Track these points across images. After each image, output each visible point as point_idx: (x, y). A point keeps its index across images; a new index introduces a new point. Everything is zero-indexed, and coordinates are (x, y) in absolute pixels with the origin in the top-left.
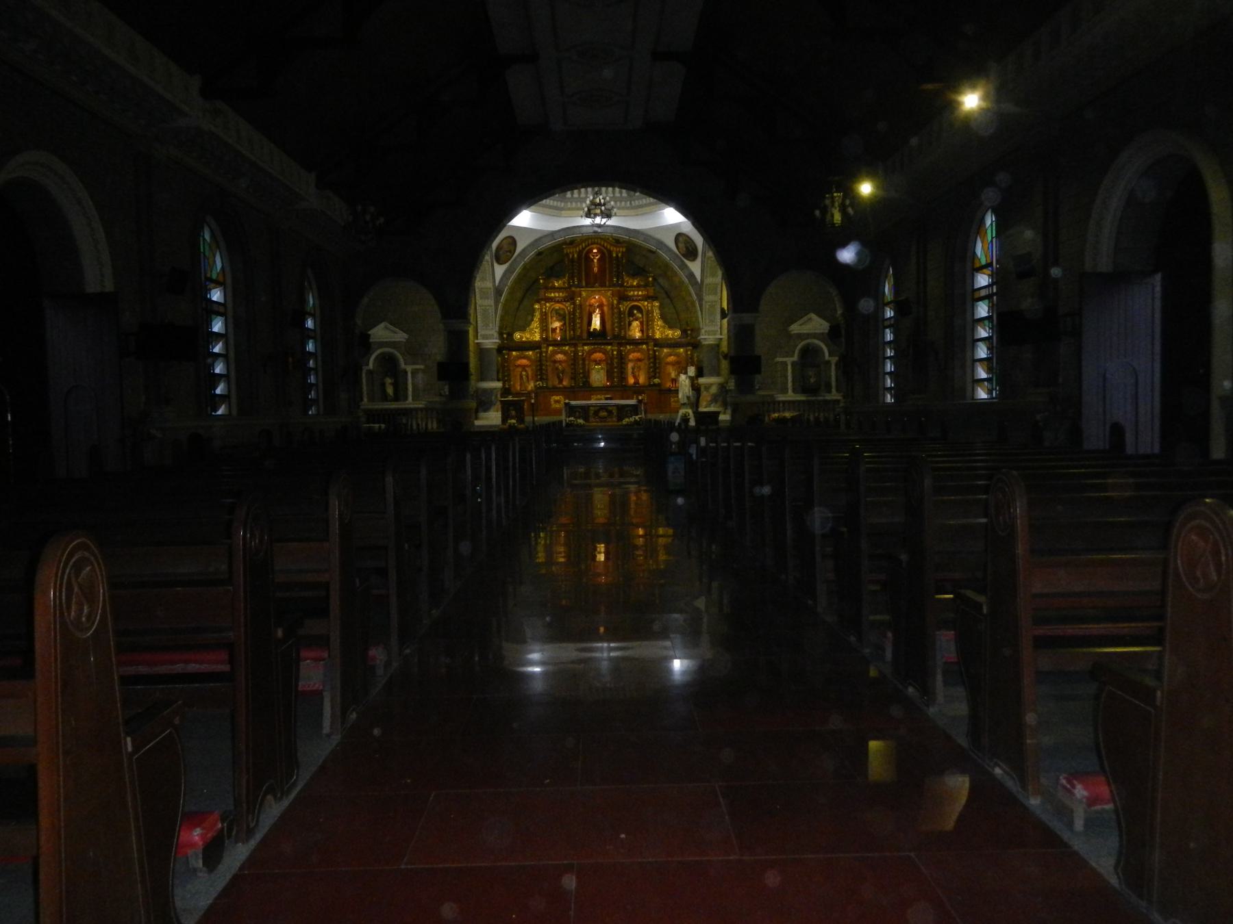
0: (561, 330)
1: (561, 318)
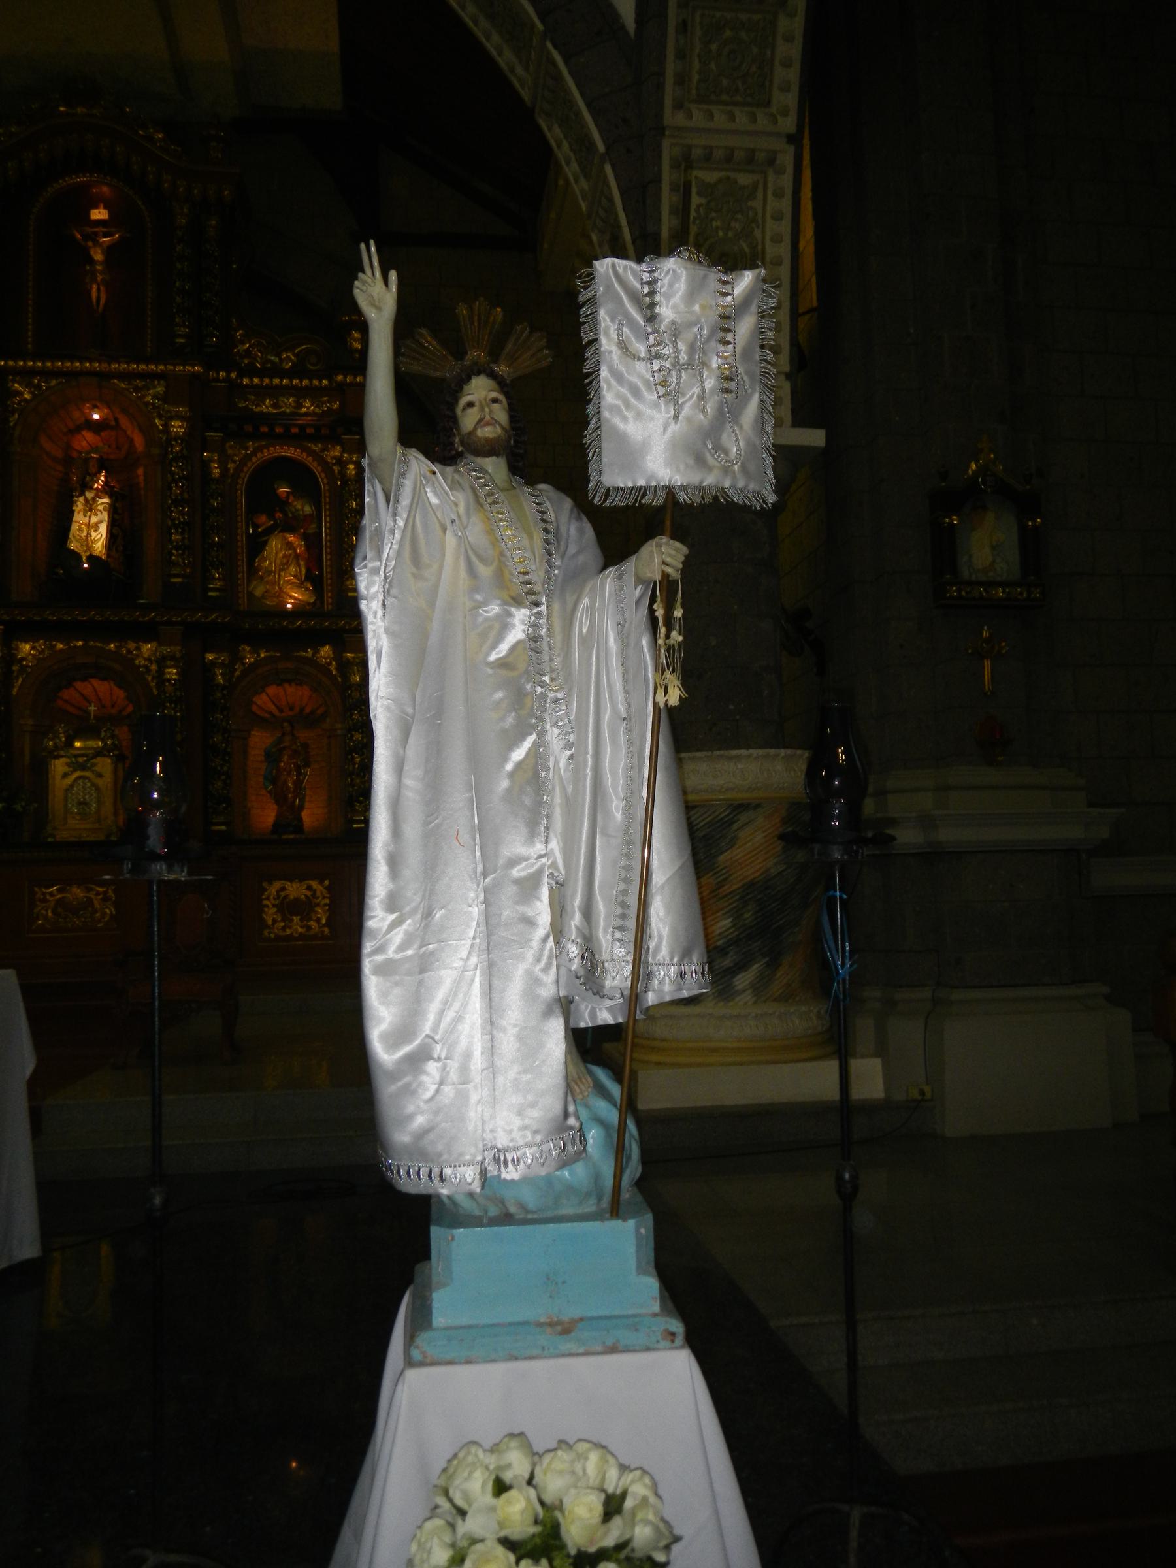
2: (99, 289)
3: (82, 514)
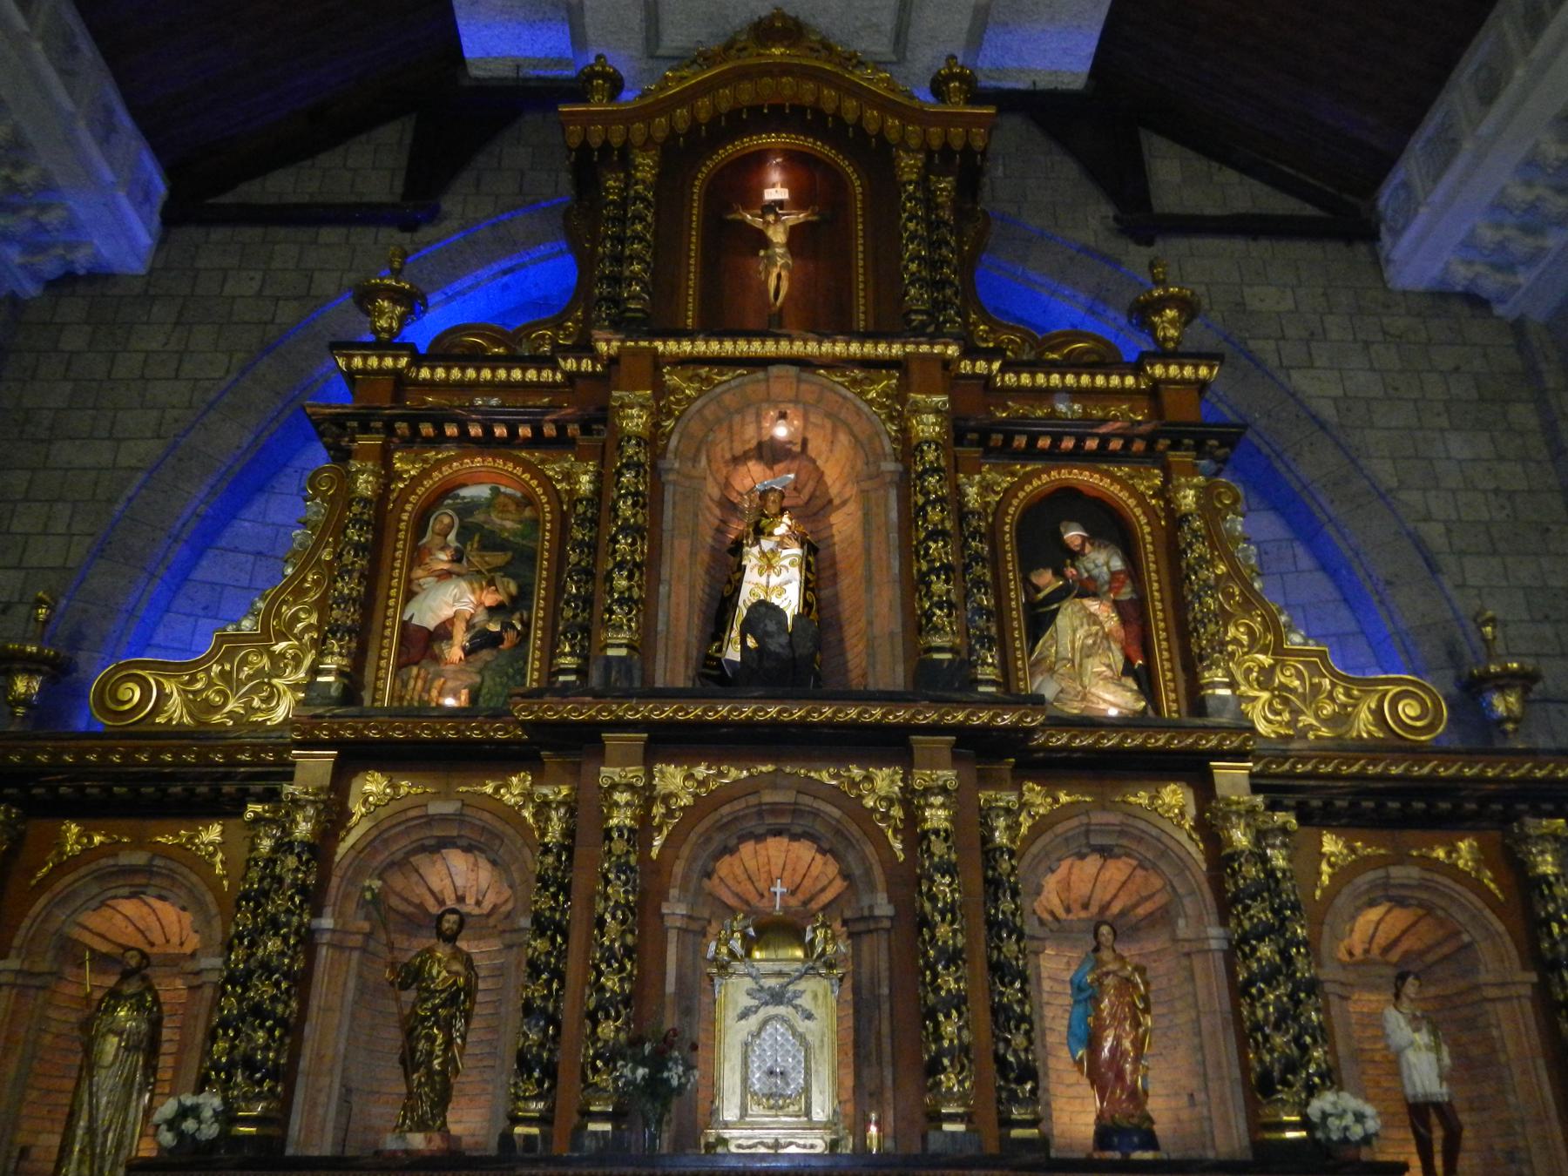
0: (482, 641)
1: (499, 558)
2: (779, 276)
3: (756, 570)
